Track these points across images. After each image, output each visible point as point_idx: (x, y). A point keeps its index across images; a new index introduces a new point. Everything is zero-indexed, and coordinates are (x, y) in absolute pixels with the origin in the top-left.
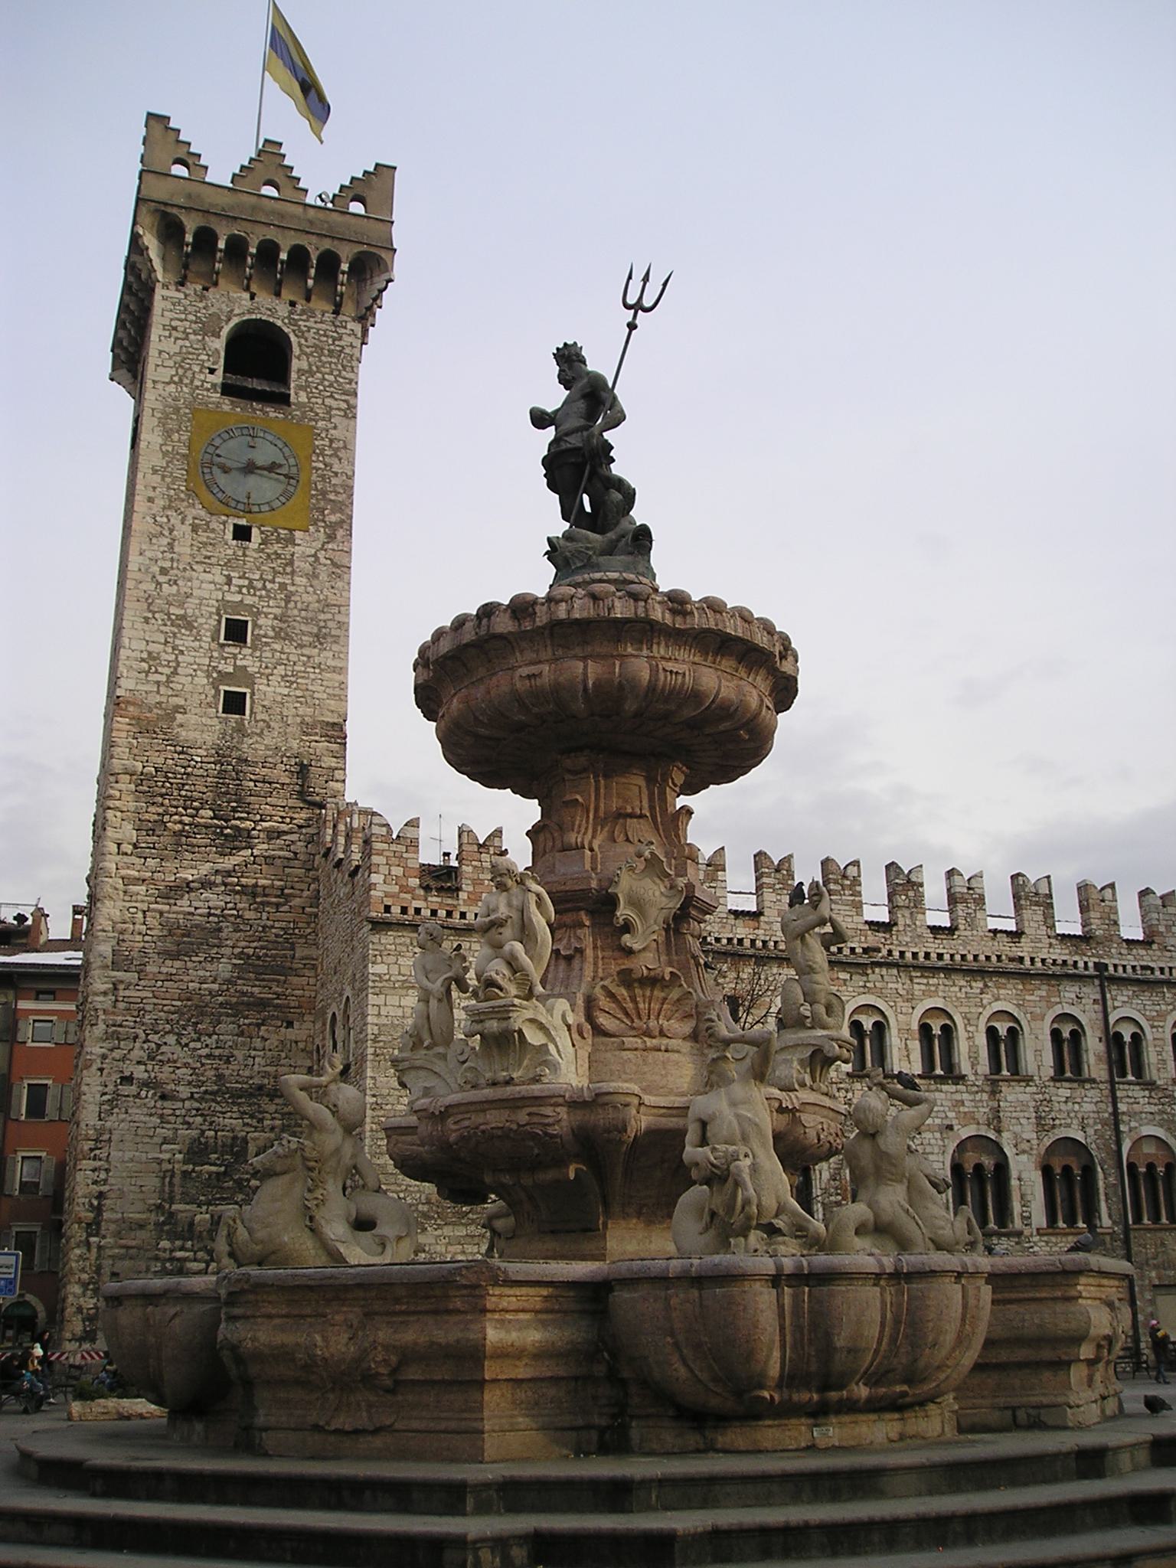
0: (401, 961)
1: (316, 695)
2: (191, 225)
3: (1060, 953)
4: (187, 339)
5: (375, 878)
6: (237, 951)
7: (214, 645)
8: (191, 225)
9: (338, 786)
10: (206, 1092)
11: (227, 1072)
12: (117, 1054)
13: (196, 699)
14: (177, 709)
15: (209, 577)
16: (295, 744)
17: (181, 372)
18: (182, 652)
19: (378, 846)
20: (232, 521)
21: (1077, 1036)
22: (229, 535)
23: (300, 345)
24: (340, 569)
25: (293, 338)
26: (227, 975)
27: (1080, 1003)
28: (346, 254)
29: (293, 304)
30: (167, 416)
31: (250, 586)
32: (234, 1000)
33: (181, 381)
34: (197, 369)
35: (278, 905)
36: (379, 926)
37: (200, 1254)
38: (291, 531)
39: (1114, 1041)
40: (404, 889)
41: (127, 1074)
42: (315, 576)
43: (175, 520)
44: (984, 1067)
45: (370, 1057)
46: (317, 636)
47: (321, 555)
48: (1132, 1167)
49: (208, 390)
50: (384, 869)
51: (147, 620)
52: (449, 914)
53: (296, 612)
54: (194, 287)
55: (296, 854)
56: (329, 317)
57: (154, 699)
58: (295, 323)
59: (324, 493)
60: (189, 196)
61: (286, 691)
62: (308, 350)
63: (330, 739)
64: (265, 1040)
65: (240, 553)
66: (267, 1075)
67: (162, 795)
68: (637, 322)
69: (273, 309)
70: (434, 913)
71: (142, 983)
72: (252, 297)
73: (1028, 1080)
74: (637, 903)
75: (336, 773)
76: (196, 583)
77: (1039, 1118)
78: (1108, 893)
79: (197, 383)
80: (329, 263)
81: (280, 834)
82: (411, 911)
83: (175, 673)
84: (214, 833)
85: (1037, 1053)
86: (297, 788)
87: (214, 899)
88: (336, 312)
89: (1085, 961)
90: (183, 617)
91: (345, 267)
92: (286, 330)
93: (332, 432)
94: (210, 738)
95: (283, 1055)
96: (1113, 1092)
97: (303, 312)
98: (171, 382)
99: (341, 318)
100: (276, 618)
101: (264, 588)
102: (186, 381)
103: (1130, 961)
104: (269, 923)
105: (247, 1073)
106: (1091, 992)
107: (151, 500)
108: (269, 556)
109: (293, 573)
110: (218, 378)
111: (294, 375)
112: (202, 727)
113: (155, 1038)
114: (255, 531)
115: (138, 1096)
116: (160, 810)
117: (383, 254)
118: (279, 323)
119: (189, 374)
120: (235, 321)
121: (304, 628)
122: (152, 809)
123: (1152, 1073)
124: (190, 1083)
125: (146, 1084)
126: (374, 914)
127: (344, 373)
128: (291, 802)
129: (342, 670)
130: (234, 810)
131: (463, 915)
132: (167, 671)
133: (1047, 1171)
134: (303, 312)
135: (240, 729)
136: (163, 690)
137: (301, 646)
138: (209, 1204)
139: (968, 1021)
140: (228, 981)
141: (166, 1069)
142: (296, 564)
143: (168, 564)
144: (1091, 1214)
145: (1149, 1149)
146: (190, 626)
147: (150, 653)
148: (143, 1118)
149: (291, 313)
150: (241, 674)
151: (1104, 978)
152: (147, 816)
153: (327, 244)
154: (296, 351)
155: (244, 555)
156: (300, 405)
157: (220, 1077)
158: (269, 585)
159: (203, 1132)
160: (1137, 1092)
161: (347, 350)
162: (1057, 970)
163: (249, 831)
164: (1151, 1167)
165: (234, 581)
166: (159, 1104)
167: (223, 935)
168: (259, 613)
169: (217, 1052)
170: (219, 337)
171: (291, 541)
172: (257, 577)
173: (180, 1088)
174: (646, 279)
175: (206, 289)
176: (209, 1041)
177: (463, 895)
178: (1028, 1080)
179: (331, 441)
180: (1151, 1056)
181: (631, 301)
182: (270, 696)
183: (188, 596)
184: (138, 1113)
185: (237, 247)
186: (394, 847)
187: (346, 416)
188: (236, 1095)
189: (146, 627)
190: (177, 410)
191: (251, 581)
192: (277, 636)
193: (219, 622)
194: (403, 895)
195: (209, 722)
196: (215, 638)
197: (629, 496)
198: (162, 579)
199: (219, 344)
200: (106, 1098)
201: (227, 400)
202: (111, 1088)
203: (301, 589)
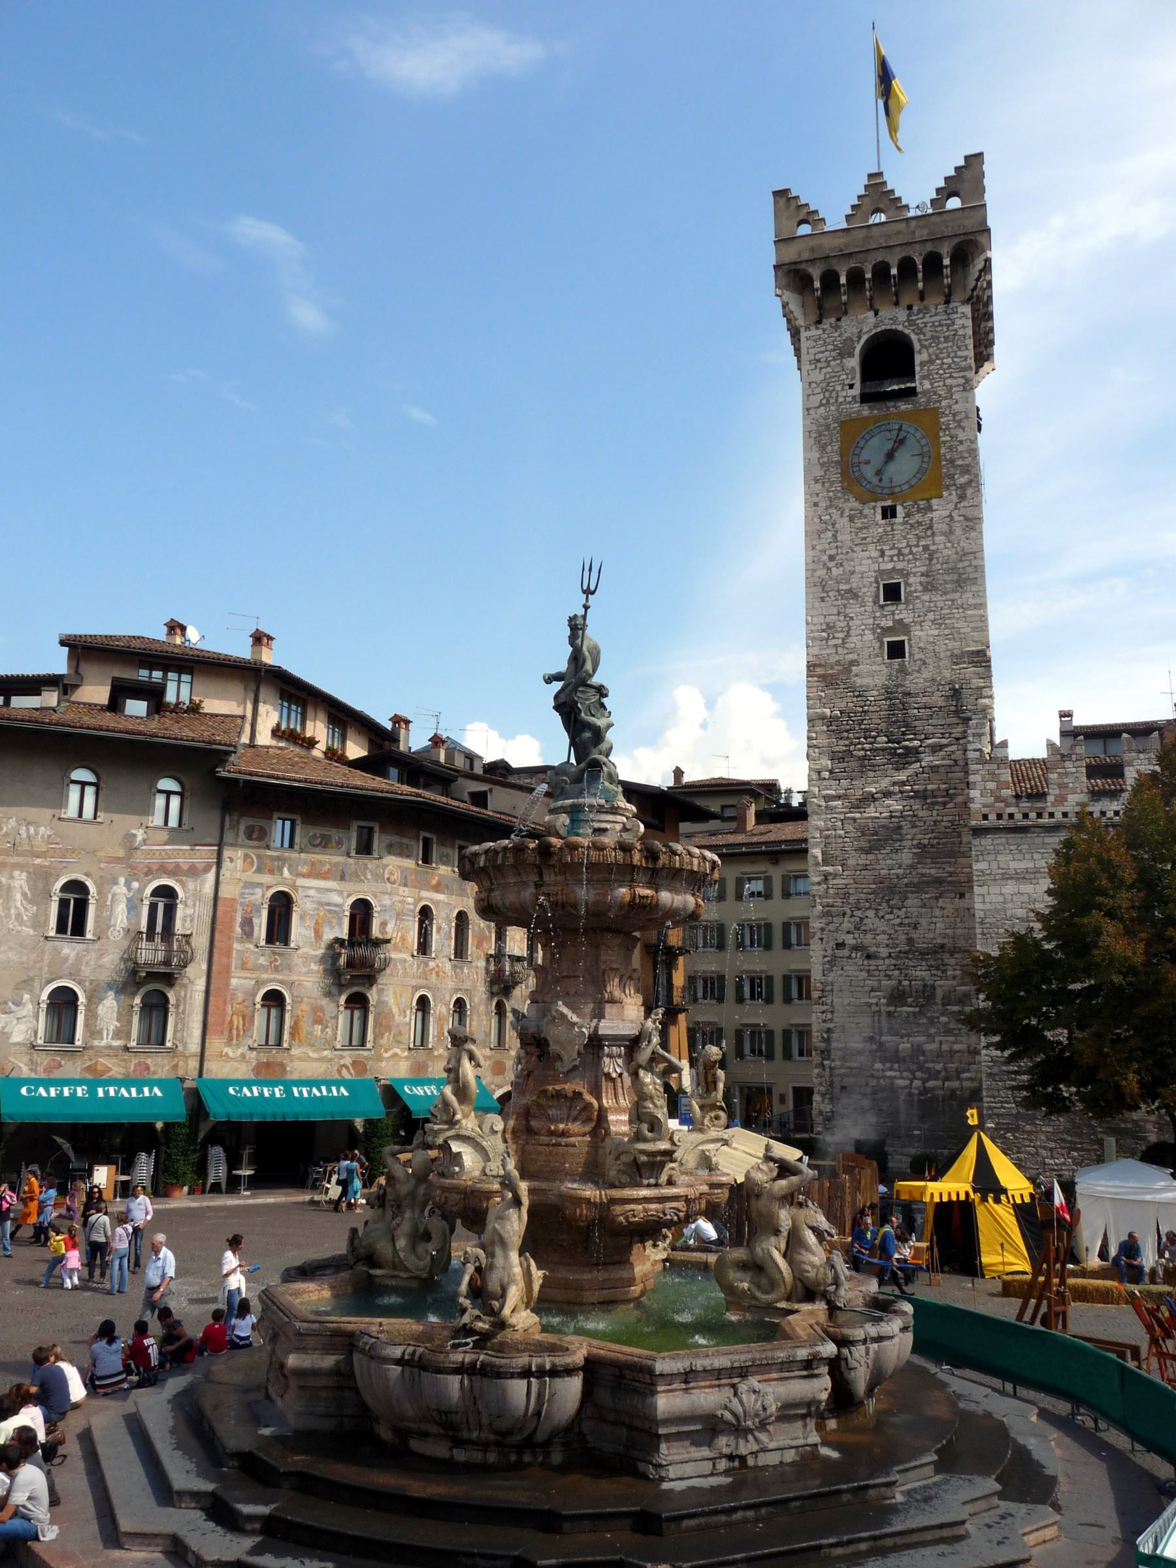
0: (1000, 858)
1: (962, 631)
2: (816, 272)
4: (829, 366)
5: (975, 793)
6: (915, 842)
7: (876, 608)
8: (816, 272)
9: (986, 701)
10: (900, 952)
11: (914, 936)
12: (831, 927)
13: (866, 652)
14: (853, 663)
17: (827, 394)
18: (852, 618)
19: (973, 767)
20: (880, 504)
22: (879, 516)
23: (919, 340)
24: (973, 523)
25: (913, 337)
26: (909, 862)
28: (945, 250)
29: (910, 307)
30: (820, 434)
31: (900, 554)
32: (916, 880)
33: (828, 402)
34: (839, 388)
35: (944, 804)
36: (978, 832)
37: (905, 1074)
38: (928, 500)
40: (999, 799)
41: (840, 941)
42: (951, 532)
43: (836, 514)
45: (979, 936)
46: (958, 582)
49: (850, 403)
50: (980, 785)
51: (823, 599)
52: (1039, 815)
53: (939, 566)
54: (828, 322)
55: (956, 761)
56: (941, 308)
58: (911, 323)
59: (952, 461)
60: (812, 250)
61: (936, 632)
62: (927, 343)
63: (976, 664)
64: (943, 908)
65: (889, 529)
66: (945, 936)
67: (847, 731)
68: (590, 603)
69: (894, 318)
70: (1026, 816)
71: (846, 873)
72: (876, 314)
79: (841, 399)
80: (933, 263)
81: (941, 747)
82: (1006, 817)
84: (890, 754)
86: (953, 708)
87: (895, 805)
88: (947, 302)
90: (850, 591)
91: (946, 262)
92: (907, 332)
93: (954, 407)
94: (880, 680)
95: (959, 920)
98: (821, 405)
99: (952, 305)
100: (922, 575)
101: (911, 553)
102: (832, 401)
104: (939, 818)
105: (931, 935)
108: (912, 526)
109: (933, 534)
110: (856, 391)
111: (917, 369)
112: (873, 673)
113: (858, 913)
114: (899, 509)
115: (850, 957)
116: (847, 742)
118: (900, 328)
119: (834, 395)
120: (865, 338)
121: (947, 578)
122: (842, 742)
124: (887, 945)
125: (855, 948)
126: (973, 823)
127: (959, 353)
128: (948, 721)
129: (982, 606)
130: (904, 734)
131: (1051, 815)
132: (841, 635)
135: (902, 670)
136: (840, 650)
137: (945, 593)
138: (909, 1036)
140: (912, 867)
141: (869, 936)
142: (935, 526)
143: (833, 552)
146: (856, 596)
147: (827, 625)
148: (855, 973)
149: (909, 316)
152: (837, 749)
153: (929, 247)
154: (917, 346)
155: (893, 530)
156: (925, 393)
157: (910, 940)
158: (915, 550)
159: (900, 982)
161: (961, 332)
163: (916, 748)
165: (887, 553)
166: (866, 962)
167: (904, 832)
168: (908, 574)
169: (906, 921)
170: (851, 355)
171: (930, 509)
172: (904, 545)
173: (881, 950)
174: (590, 570)
175: (839, 320)
176: (899, 913)
177: (1050, 798)
179: (954, 415)
181: (585, 588)
182: (924, 638)
183: (853, 573)
184: (851, 969)
185: (856, 278)
186: (987, 767)
187: (965, 390)
188: (923, 954)
189: (823, 604)
190: (828, 427)
191: (900, 550)
193: (878, 588)
194: (998, 804)
195: (878, 668)
196: (876, 602)
198: (831, 564)
199: (854, 362)
200: (826, 959)
202: (829, 952)
203: (941, 547)
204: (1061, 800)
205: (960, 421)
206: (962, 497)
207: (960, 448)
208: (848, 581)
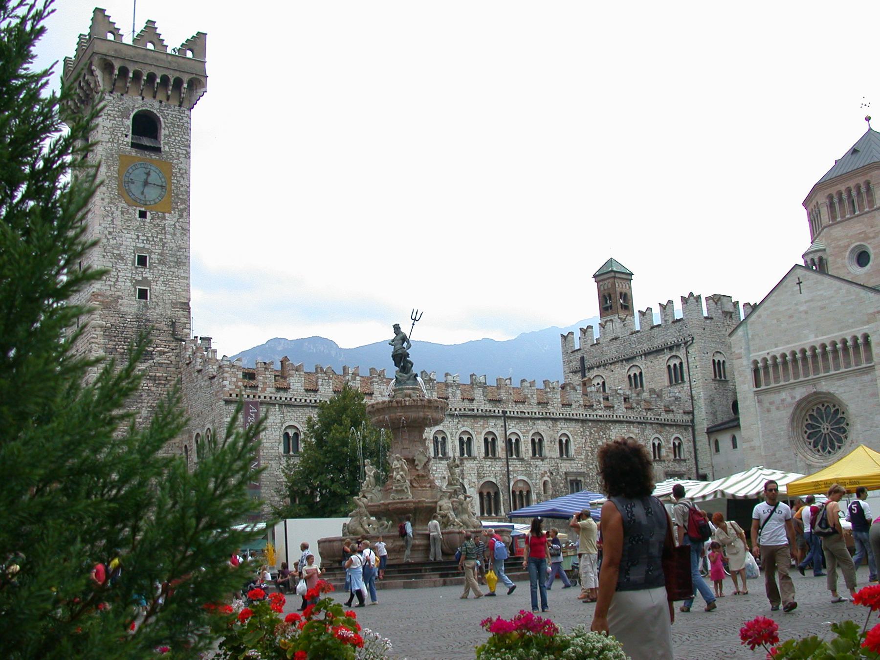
2: (117, 65)
3: (488, 407)
7: (133, 268)
9: (187, 331)
13: (126, 293)
14: (119, 297)
15: (129, 236)
16: (169, 312)
20: (138, 209)
21: (494, 440)
22: (137, 216)
24: (186, 231)
25: (161, 119)
27: (495, 427)
28: (186, 78)
29: (161, 102)
31: (147, 240)
34: (120, 135)
35: (165, 384)
38: (164, 213)
39: (509, 442)
40: (237, 387)
42: (175, 234)
43: (114, 209)
44: (458, 454)
47: (177, 224)
48: (513, 492)
50: (229, 379)
51: (104, 256)
54: (116, 94)
56: (177, 108)
57: (108, 293)
58: (162, 111)
59: (177, 195)
60: (116, 51)
63: (184, 310)
69: (152, 105)
73: (475, 458)
74: (420, 461)
75: (187, 325)
76: (124, 239)
77: (478, 473)
78: (508, 382)
81: (165, 353)
83: (117, 281)
85: (479, 447)
88: (180, 106)
89: (498, 410)
90: (119, 255)
94: (134, 310)
96: (507, 463)
97: (166, 106)
103: (516, 409)
106: (501, 423)
107: (103, 199)
110: (129, 140)
111: (163, 138)
114: (148, 214)
117: (202, 79)
120: (136, 110)
121: (171, 259)
123: (523, 455)
128: (168, 339)
129: (188, 278)
131: (259, 397)
132: (114, 280)
133: (481, 494)
134: (166, 106)
135: (146, 306)
137: (170, 267)
139: (451, 434)
143: (111, 230)
144: (497, 511)
145: (521, 485)
146: (122, 259)
150: (145, 281)
151: (505, 417)
153: (177, 74)
154: (163, 125)
160: (517, 463)
162: (487, 414)
163: (151, 352)
164: (521, 492)
168: (152, 252)
171: (164, 218)
175: (122, 95)
177: (259, 389)
178: (475, 458)
180: (522, 448)
183: (121, 245)
185: (137, 75)
190: (112, 155)
192: (159, 263)
196: (133, 264)
197: (412, 365)
198: (109, 237)
199: (129, 122)
201: (134, 150)
204: (264, 390)
205: (182, 174)
206: (181, 216)
207: (182, 189)
208: (118, 249)
